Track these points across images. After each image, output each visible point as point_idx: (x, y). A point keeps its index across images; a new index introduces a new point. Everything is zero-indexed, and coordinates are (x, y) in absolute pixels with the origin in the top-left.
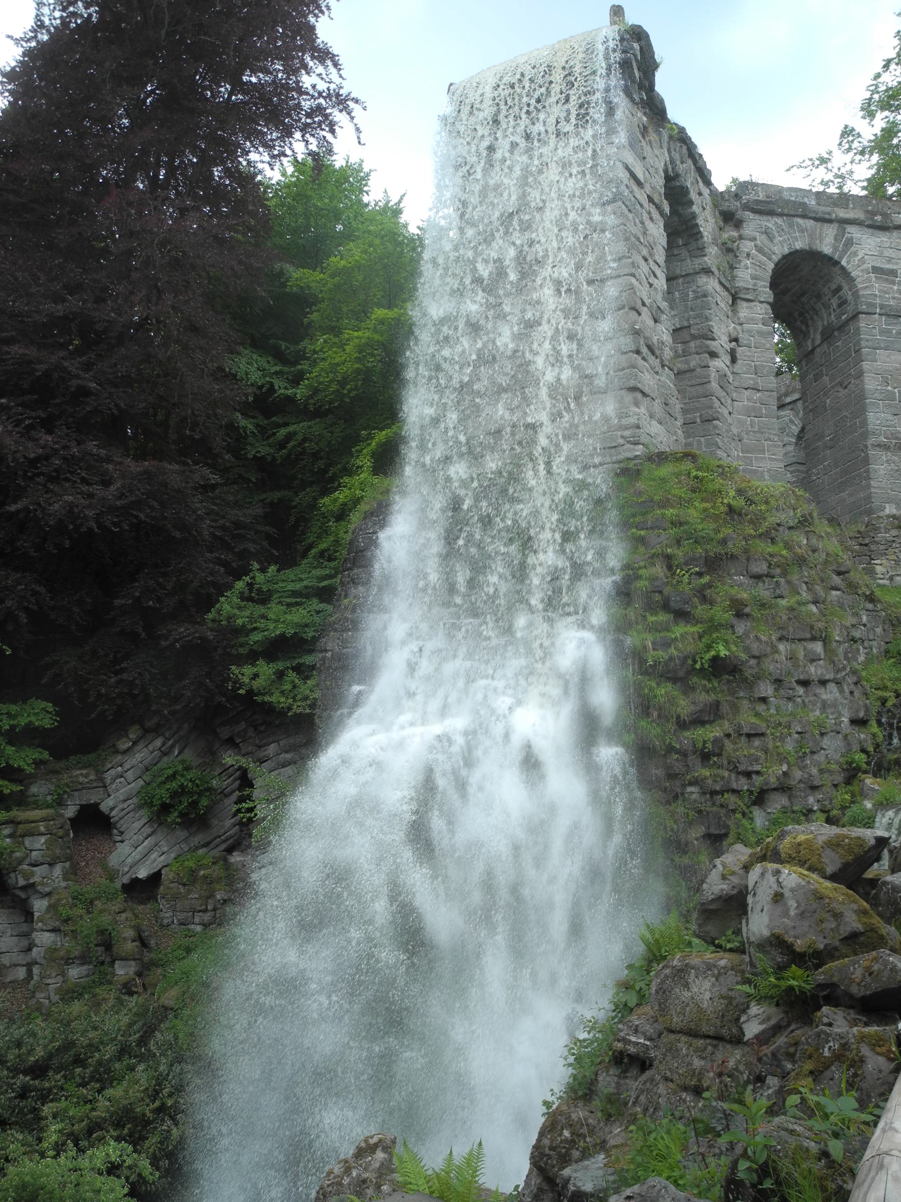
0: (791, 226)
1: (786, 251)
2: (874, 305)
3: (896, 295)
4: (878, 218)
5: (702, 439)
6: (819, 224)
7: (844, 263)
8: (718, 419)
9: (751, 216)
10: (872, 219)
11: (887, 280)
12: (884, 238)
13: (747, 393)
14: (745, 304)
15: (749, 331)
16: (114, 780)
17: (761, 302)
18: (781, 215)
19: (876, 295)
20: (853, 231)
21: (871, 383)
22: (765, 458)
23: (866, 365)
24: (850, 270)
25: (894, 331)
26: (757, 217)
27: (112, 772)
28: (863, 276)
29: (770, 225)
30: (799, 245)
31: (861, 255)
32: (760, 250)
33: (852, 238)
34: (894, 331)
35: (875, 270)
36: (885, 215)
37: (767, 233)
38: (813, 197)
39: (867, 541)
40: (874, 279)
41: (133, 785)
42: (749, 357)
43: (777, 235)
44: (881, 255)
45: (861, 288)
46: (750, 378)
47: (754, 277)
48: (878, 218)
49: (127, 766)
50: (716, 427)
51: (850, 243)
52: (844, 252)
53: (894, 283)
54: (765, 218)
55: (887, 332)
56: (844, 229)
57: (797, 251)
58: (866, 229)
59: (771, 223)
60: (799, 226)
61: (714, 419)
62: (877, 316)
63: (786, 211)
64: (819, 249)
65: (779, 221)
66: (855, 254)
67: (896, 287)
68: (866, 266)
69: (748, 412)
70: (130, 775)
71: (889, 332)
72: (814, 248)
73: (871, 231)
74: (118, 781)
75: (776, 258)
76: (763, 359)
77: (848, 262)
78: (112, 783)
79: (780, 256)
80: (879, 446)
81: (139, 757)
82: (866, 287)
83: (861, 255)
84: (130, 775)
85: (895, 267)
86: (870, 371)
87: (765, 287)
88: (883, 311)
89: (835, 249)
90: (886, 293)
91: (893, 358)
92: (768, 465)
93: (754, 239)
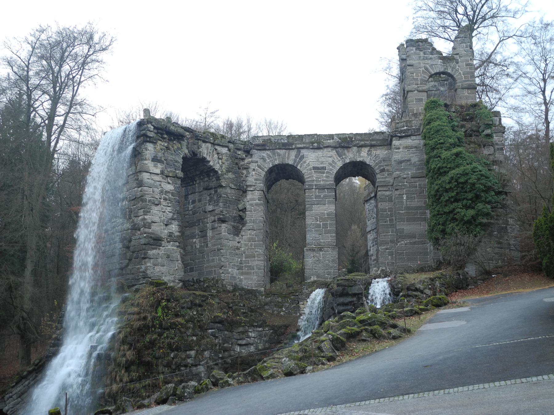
0: (274, 154)
1: (271, 166)
2: (312, 185)
3: (325, 179)
4: (316, 145)
5: (217, 258)
6: (288, 151)
7: (299, 167)
8: (222, 249)
9: (256, 151)
10: (313, 145)
11: (320, 172)
12: (320, 153)
13: (249, 232)
14: (250, 192)
15: (252, 205)
16: (8, 399)
17: (258, 191)
18: (269, 150)
19: (314, 180)
20: (304, 152)
21: (309, 221)
22: (255, 260)
23: (307, 213)
24: (301, 170)
25: (322, 196)
26: (259, 152)
27: (8, 396)
28: (308, 172)
29: (264, 155)
30: (277, 162)
31: (307, 162)
32: (259, 167)
33: (304, 155)
34: (322, 196)
35: (314, 168)
36: (319, 143)
37: (264, 159)
38: (286, 139)
39: (297, 294)
40: (313, 173)
41: (16, 401)
42: (250, 216)
43: (267, 159)
44: (318, 161)
45: (306, 178)
46: (251, 225)
47: (256, 180)
48: (316, 145)
49: (14, 393)
50: (221, 253)
51: (303, 157)
52: (299, 162)
53: (324, 173)
54: (262, 152)
55: (319, 196)
56: (300, 151)
57: (276, 165)
58: (311, 150)
59: (264, 154)
60: (277, 153)
61: (221, 249)
62: (314, 190)
63: (271, 148)
64: (287, 162)
65: (268, 152)
66: (305, 162)
67: (324, 175)
68: (310, 167)
69: (249, 240)
70: (15, 397)
71: (319, 196)
72: (284, 163)
73: (313, 150)
74: (10, 399)
75: (266, 170)
76: (257, 216)
77: (301, 167)
78: (7, 400)
79: (268, 169)
80: (310, 250)
81: (19, 389)
82: (309, 177)
83: (307, 162)
84: (15, 397)
85: (325, 165)
86: (309, 216)
87: (260, 183)
88: (317, 187)
89: (295, 161)
90: (319, 178)
91: (321, 208)
92: (257, 263)
93: (257, 162)
